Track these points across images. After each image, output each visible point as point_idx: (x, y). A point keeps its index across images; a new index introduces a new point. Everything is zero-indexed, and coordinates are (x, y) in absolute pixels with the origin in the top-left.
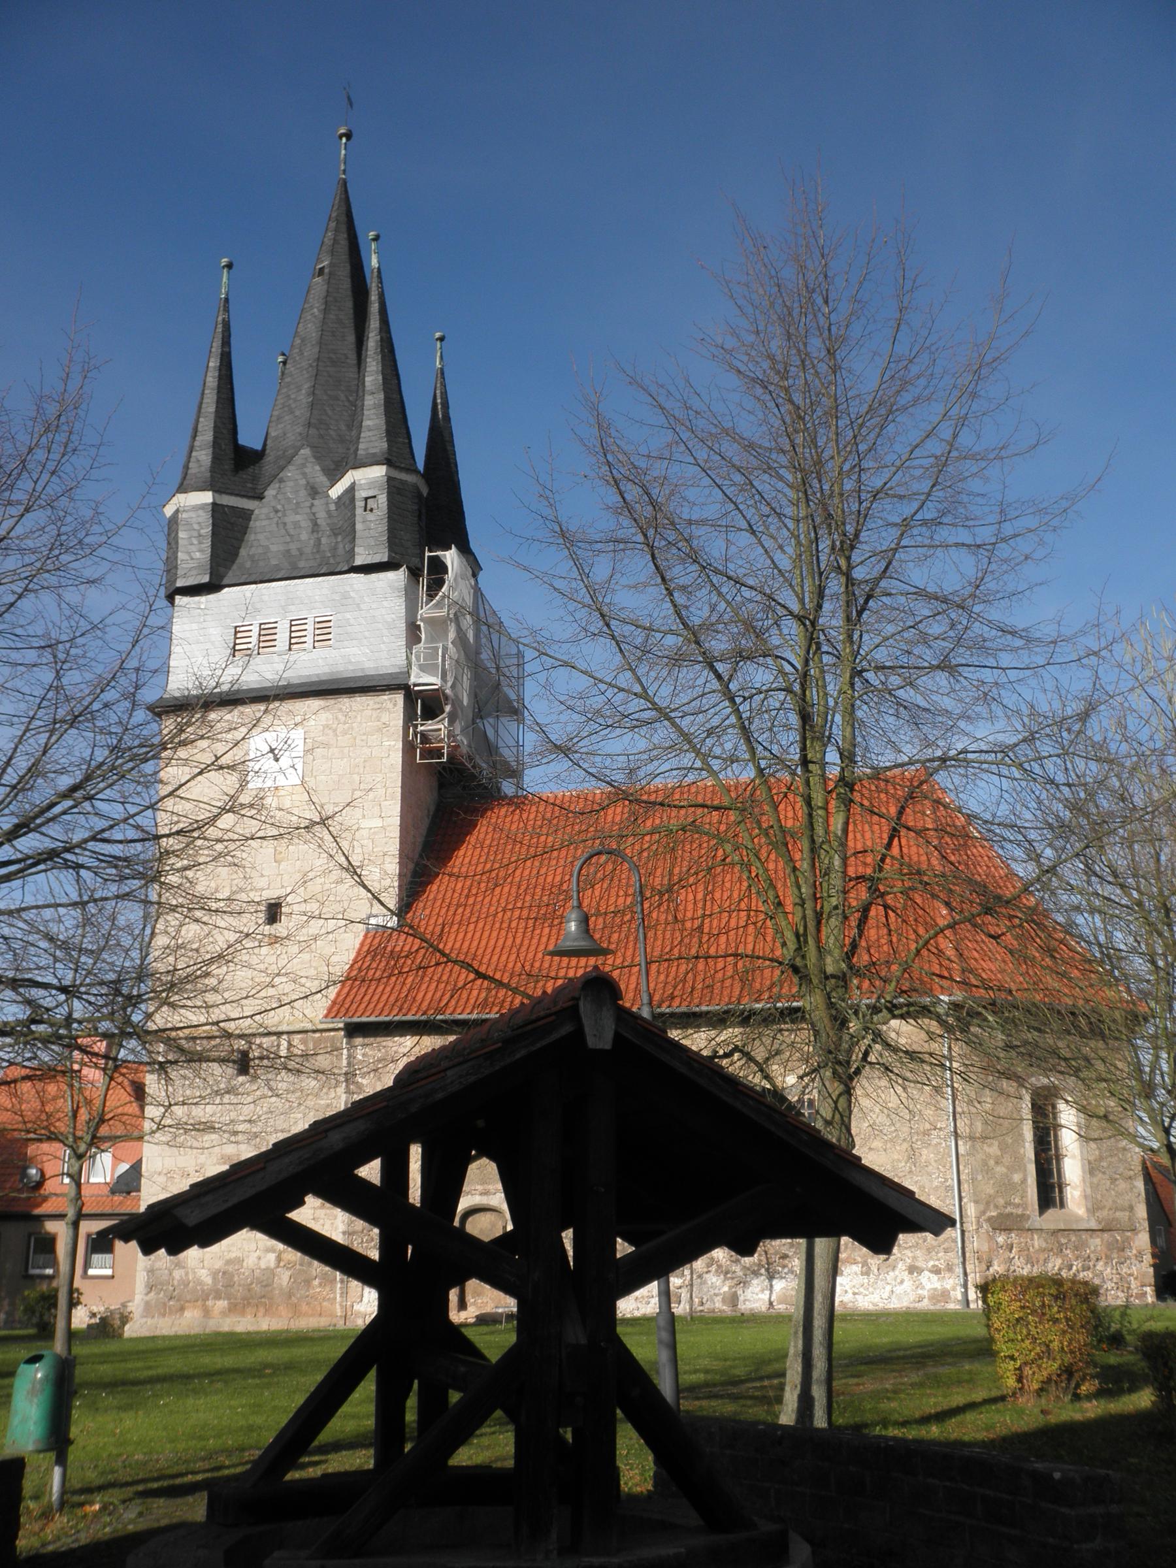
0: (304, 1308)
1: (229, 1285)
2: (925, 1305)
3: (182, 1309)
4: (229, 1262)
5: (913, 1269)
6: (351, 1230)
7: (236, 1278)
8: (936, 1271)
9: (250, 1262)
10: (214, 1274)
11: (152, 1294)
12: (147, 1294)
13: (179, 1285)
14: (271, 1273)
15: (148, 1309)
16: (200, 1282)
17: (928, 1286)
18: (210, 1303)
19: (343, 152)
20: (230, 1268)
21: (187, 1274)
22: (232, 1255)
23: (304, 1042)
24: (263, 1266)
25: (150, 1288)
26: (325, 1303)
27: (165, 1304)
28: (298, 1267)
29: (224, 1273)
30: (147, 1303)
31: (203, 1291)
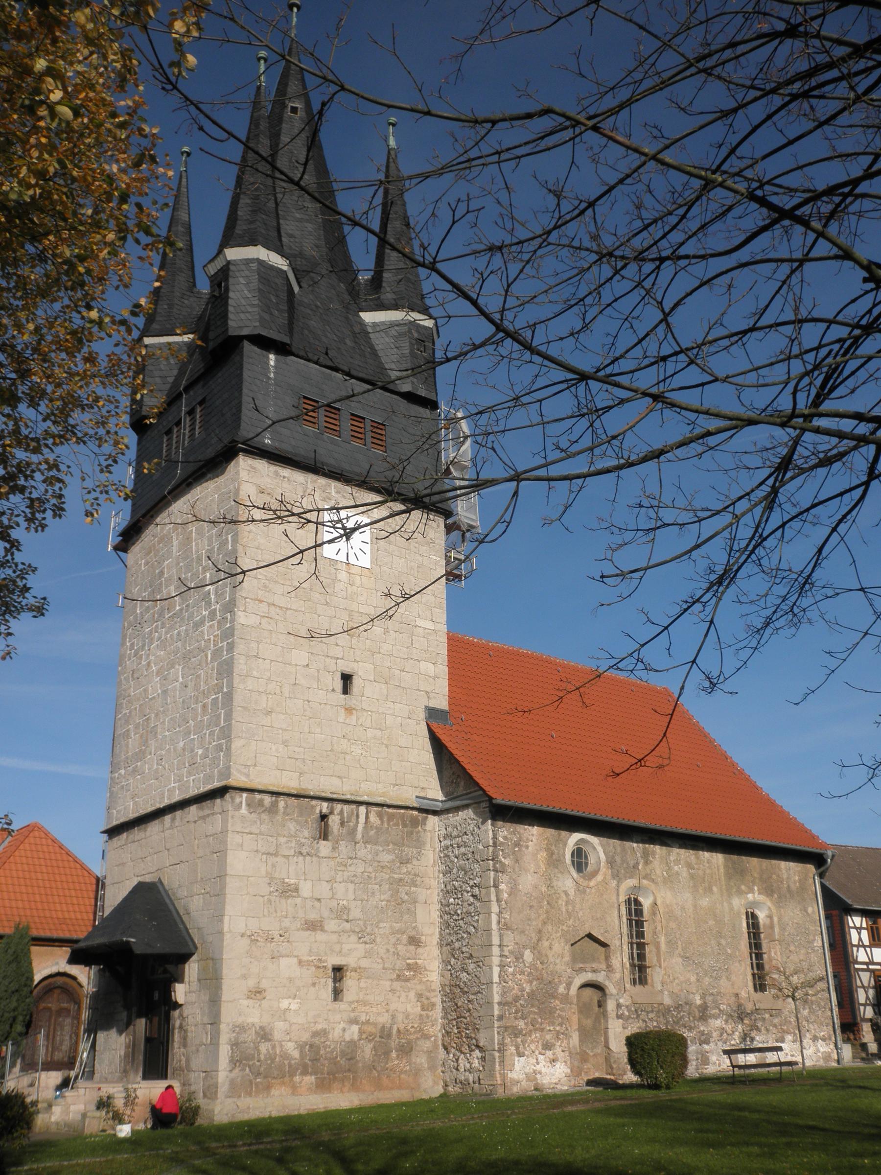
0: (385, 1081)
1: (315, 1060)
2: (821, 1063)
3: (268, 1088)
4: (316, 1034)
5: (815, 1039)
6: (504, 1001)
7: (322, 1052)
8: (824, 1040)
9: (336, 1034)
10: (301, 1047)
11: (237, 1070)
12: (231, 1071)
13: (266, 1060)
14: (352, 1044)
15: (235, 1089)
16: (285, 1056)
17: (822, 1050)
18: (297, 1079)
19: (295, 19)
20: (316, 1041)
21: (274, 1047)
22: (319, 1027)
23: (380, 816)
24: (348, 1039)
25: (234, 1062)
26: (403, 1076)
27: (251, 1081)
28: (377, 1039)
29: (311, 1046)
30: (232, 1082)
31: (290, 1065)
